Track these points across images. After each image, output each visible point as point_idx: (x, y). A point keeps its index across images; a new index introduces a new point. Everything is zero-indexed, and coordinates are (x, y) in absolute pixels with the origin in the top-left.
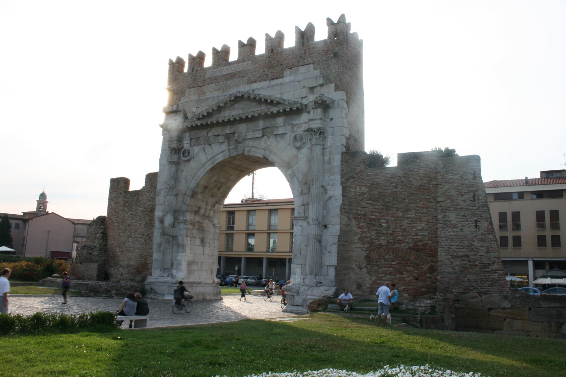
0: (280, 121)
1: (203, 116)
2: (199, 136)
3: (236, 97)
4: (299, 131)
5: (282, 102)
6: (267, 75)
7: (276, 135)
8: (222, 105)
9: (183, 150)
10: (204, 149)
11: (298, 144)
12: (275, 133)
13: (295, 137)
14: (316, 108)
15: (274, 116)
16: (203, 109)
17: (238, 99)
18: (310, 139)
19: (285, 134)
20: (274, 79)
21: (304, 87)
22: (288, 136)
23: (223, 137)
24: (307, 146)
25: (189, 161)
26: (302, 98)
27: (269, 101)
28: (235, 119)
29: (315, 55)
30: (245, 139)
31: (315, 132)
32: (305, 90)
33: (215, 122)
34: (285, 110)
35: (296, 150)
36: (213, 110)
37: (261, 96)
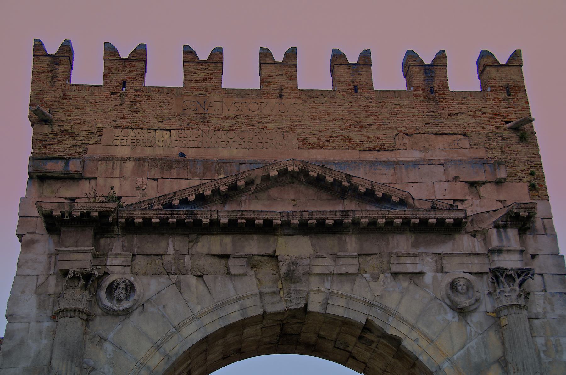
0: (402, 243)
1: (184, 202)
2: (161, 251)
3: (284, 173)
4: (458, 271)
5: (411, 201)
6: (350, 139)
7: (395, 274)
8: (241, 183)
9: (107, 282)
10: (178, 284)
11: (464, 301)
12: (394, 269)
13: (453, 286)
14: (505, 227)
15: (390, 228)
16: (182, 185)
17: (287, 178)
18: (490, 294)
19: (421, 274)
20: (370, 149)
21: (456, 178)
22: (428, 279)
23: (243, 262)
24: (482, 309)
25: (127, 313)
26: (454, 201)
27: (380, 194)
28: (286, 224)
29: (463, 116)
30: (309, 274)
31: (510, 278)
32: (458, 185)
33: (224, 221)
34: (424, 222)
35: (456, 314)
36: (216, 192)
37: (354, 180)
